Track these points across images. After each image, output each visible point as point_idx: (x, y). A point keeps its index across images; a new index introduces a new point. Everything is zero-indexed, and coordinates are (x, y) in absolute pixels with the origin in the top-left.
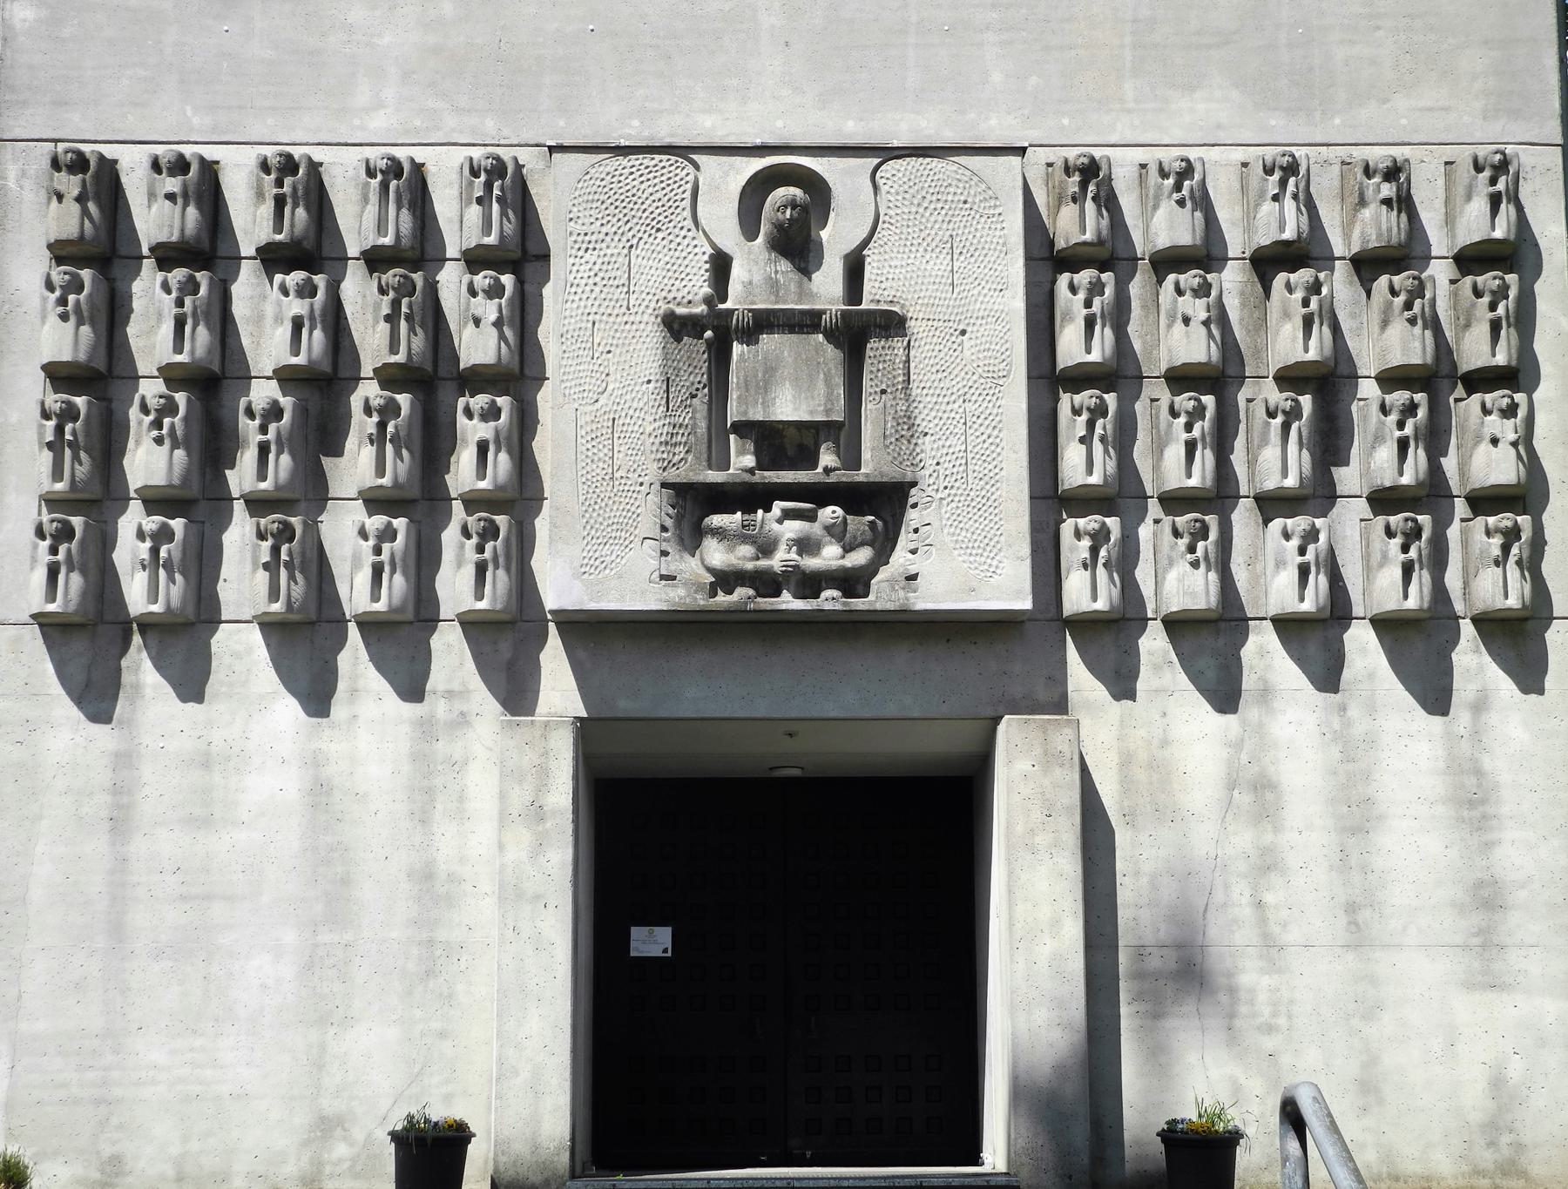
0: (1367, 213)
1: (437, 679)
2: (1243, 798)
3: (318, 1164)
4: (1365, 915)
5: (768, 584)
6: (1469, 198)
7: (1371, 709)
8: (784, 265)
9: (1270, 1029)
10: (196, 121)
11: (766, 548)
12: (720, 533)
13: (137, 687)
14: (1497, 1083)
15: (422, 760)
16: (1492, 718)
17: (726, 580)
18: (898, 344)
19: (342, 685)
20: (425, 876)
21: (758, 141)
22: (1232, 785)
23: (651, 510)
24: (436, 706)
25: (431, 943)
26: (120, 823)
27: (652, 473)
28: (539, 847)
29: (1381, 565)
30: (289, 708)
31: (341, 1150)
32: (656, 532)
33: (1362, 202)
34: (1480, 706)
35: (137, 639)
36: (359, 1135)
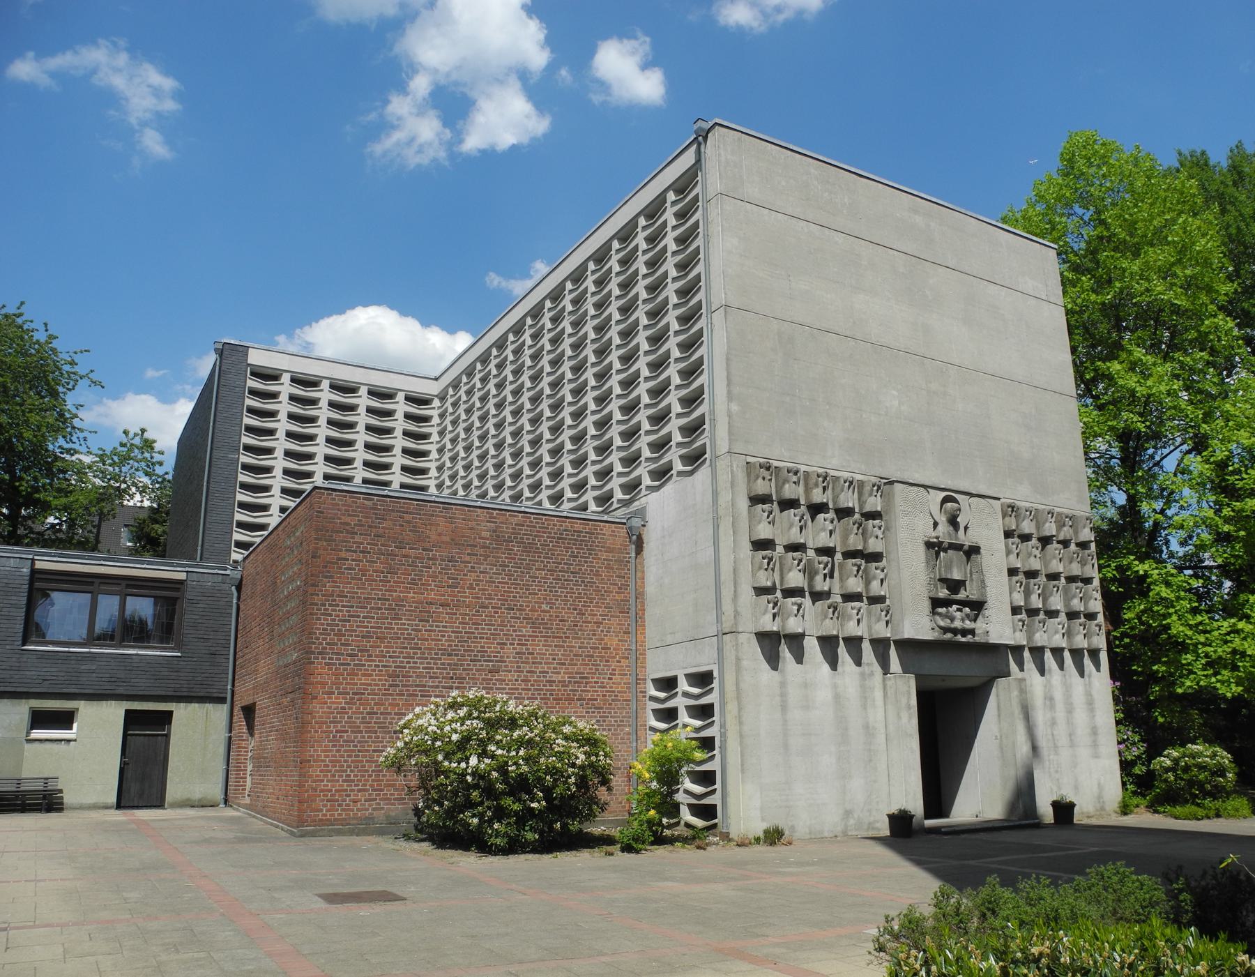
0: (1065, 529)
1: (864, 660)
2: (1048, 703)
3: (846, 826)
4: (1073, 737)
5: (955, 631)
6: (1084, 527)
7: (1070, 676)
8: (951, 528)
9: (1057, 772)
10: (785, 454)
11: (952, 619)
12: (940, 614)
13: (784, 658)
14: (1099, 784)
15: (863, 687)
16: (1092, 679)
17: (945, 630)
18: (979, 556)
19: (840, 660)
20: (867, 727)
21: (943, 486)
22: (1045, 699)
23: (926, 605)
24: (865, 668)
25: (870, 750)
26: (784, 708)
27: (926, 595)
28: (910, 718)
29: (1077, 634)
30: (826, 667)
31: (852, 822)
32: (929, 613)
33: (1064, 525)
34: (1090, 676)
35: (783, 641)
36: (856, 816)
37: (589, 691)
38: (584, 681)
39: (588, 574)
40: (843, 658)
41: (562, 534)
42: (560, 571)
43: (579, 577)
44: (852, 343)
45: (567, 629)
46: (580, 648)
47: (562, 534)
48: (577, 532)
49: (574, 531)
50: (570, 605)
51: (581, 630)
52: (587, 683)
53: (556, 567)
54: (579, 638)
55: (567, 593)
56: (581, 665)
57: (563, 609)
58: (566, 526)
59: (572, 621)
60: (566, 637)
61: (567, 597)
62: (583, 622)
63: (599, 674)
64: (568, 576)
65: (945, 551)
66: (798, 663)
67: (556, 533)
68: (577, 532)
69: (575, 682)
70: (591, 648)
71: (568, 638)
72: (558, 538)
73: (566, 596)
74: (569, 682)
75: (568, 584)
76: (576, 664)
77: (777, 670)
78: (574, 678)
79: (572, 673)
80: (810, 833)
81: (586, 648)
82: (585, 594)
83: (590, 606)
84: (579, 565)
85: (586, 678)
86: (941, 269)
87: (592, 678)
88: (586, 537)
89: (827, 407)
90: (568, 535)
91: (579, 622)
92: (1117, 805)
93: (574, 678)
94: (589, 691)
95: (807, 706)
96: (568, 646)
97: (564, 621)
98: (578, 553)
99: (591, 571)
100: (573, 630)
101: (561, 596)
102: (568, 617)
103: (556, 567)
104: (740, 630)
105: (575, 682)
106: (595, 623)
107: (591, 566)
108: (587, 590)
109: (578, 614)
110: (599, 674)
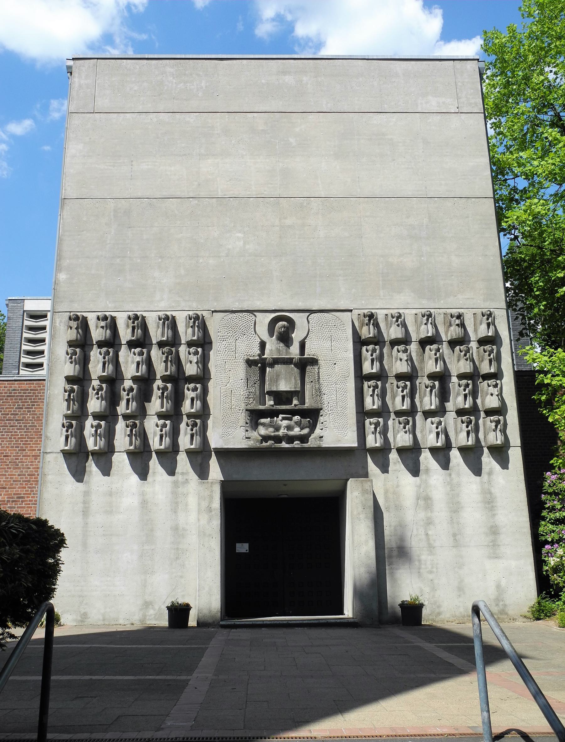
0: (452, 328)
1: (179, 469)
2: (421, 502)
3: (145, 616)
4: (458, 537)
5: (278, 439)
6: (481, 324)
7: (458, 475)
8: (282, 345)
9: (431, 572)
10: (110, 305)
11: (277, 429)
12: (263, 424)
13: (90, 472)
14: (498, 586)
15: (175, 494)
16: (494, 477)
17: (265, 438)
18: (316, 367)
19: (150, 471)
20: (176, 529)
21: (274, 309)
22: (418, 499)
23: (242, 417)
24: (178, 477)
25: (178, 549)
26: (86, 512)
27: (243, 407)
28: (210, 520)
29: (460, 432)
30: (135, 478)
31: (151, 612)
32: (244, 424)
33: (451, 325)
34: (490, 473)
35: (90, 457)
36: (157, 607)
37: (24, 507)
38: (21, 500)
39: (30, 420)
40: (154, 469)
41: (11, 393)
42: (7, 420)
43: (23, 423)
44: (195, 202)
45: (10, 462)
46: (19, 475)
47: (11, 393)
48: (23, 390)
49: (21, 390)
50: (14, 444)
51: (21, 462)
52: (22, 502)
53: (4, 417)
54: (19, 468)
55: (12, 435)
56: (19, 488)
57: (7, 447)
58: (15, 387)
59: (14, 456)
60: (8, 468)
61: (11, 438)
62: (23, 456)
63: (33, 494)
64: (14, 423)
65: (272, 365)
66: (104, 475)
67: (6, 393)
68: (23, 390)
69: (13, 501)
70: (28, 475)
71: (10, 468)
72: (8, 396)
73: (10, 438)
74: (8, 501)
75: (12, 429)
76: (15, 488)
77: (82, 482)
78: (13, 498)
79: (11, 494)
80: (104, 620)
81: (25, 475)
82: (26, 435)
83: (30, 444)
84: (23, 414)
85: (23, 497)
86: (311, 116)
87: (28, 497)
88: (30, 393)
89: (160, 260)
90: (16, 393)
91: (19, 456)
92: (527, 609)
93: (13, 498)
94: (24, 507)
95: (110, 510)
96: (9, 475)
97: (7, 456)
98: (23, 405)
99: (33, 418)
100: (14, 462)
101: (6, 438)
102: (11, 453)
103: (4, 417)
104: (48, 451)
105: (13, 501)
106: (33, 456)
107: (33, 414)
108: (28, 432)
109: (19, 450)
110: (33, 494)
